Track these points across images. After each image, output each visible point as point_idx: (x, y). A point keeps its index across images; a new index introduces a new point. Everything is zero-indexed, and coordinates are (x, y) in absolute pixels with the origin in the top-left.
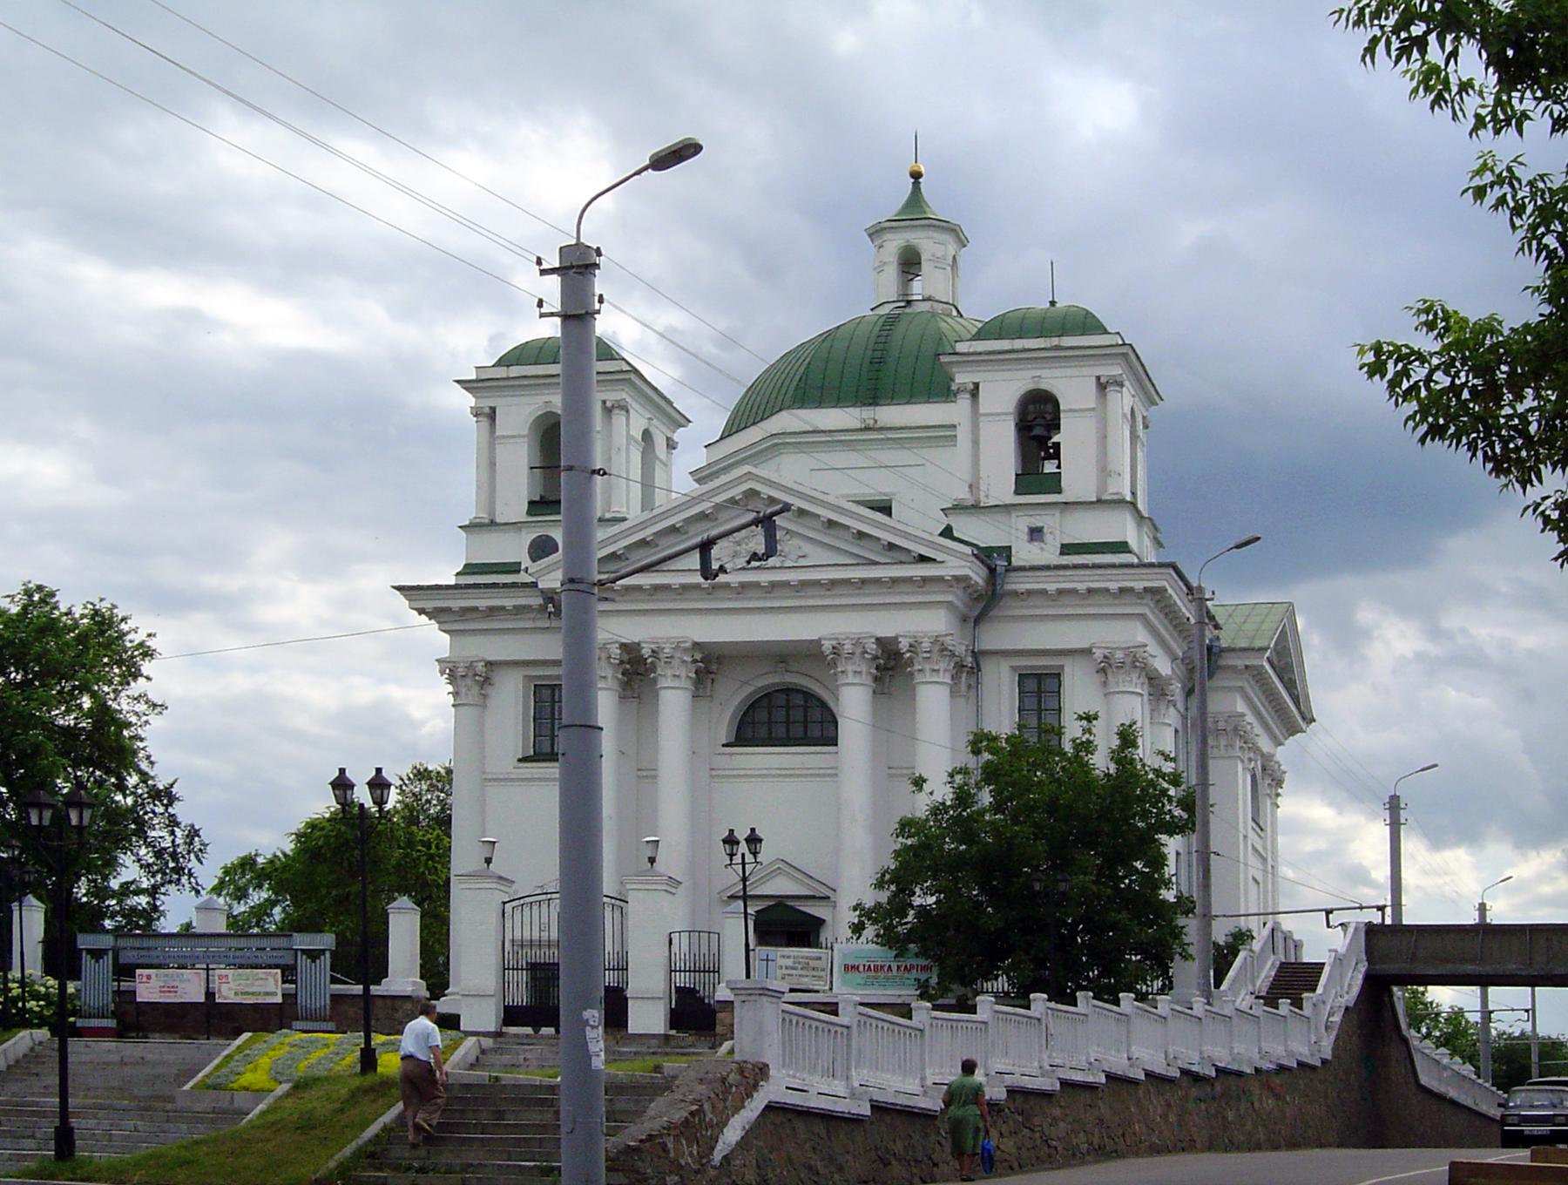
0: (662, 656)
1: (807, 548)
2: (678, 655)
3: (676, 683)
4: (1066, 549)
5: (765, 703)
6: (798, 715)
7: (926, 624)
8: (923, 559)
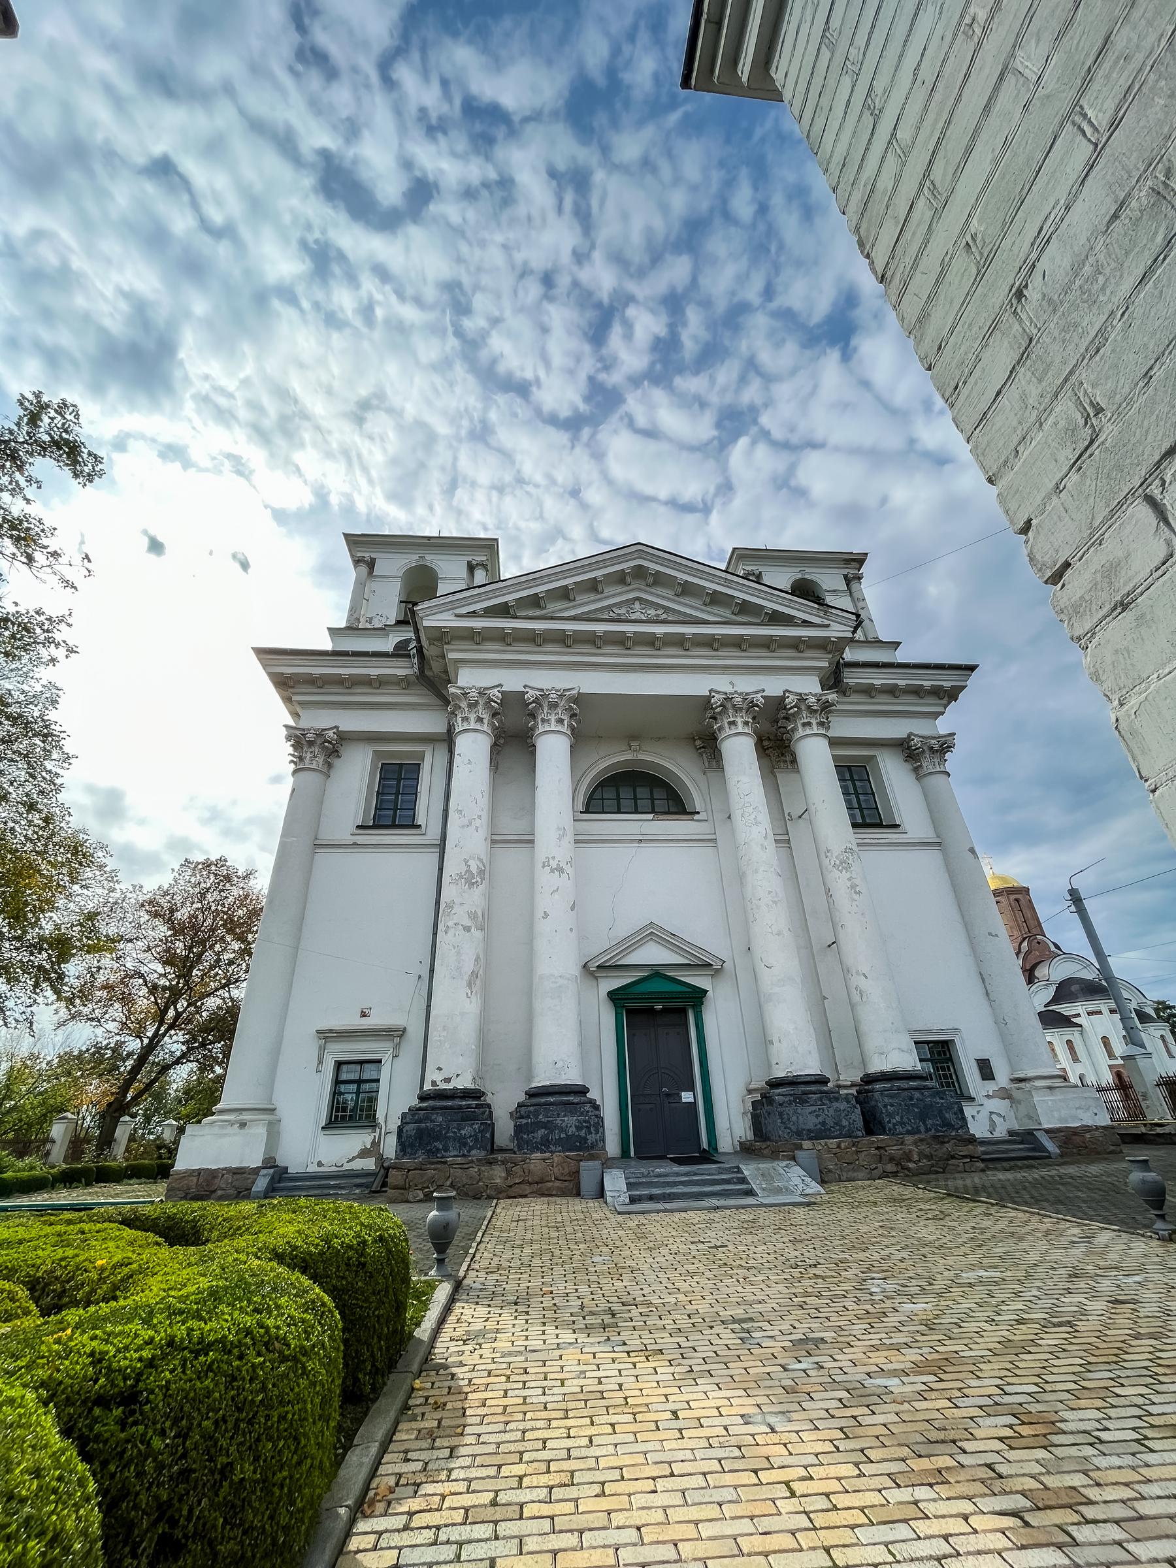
0: (545, 705)
3: (560, 728)
7: (809, 686)
8: (806, 623)
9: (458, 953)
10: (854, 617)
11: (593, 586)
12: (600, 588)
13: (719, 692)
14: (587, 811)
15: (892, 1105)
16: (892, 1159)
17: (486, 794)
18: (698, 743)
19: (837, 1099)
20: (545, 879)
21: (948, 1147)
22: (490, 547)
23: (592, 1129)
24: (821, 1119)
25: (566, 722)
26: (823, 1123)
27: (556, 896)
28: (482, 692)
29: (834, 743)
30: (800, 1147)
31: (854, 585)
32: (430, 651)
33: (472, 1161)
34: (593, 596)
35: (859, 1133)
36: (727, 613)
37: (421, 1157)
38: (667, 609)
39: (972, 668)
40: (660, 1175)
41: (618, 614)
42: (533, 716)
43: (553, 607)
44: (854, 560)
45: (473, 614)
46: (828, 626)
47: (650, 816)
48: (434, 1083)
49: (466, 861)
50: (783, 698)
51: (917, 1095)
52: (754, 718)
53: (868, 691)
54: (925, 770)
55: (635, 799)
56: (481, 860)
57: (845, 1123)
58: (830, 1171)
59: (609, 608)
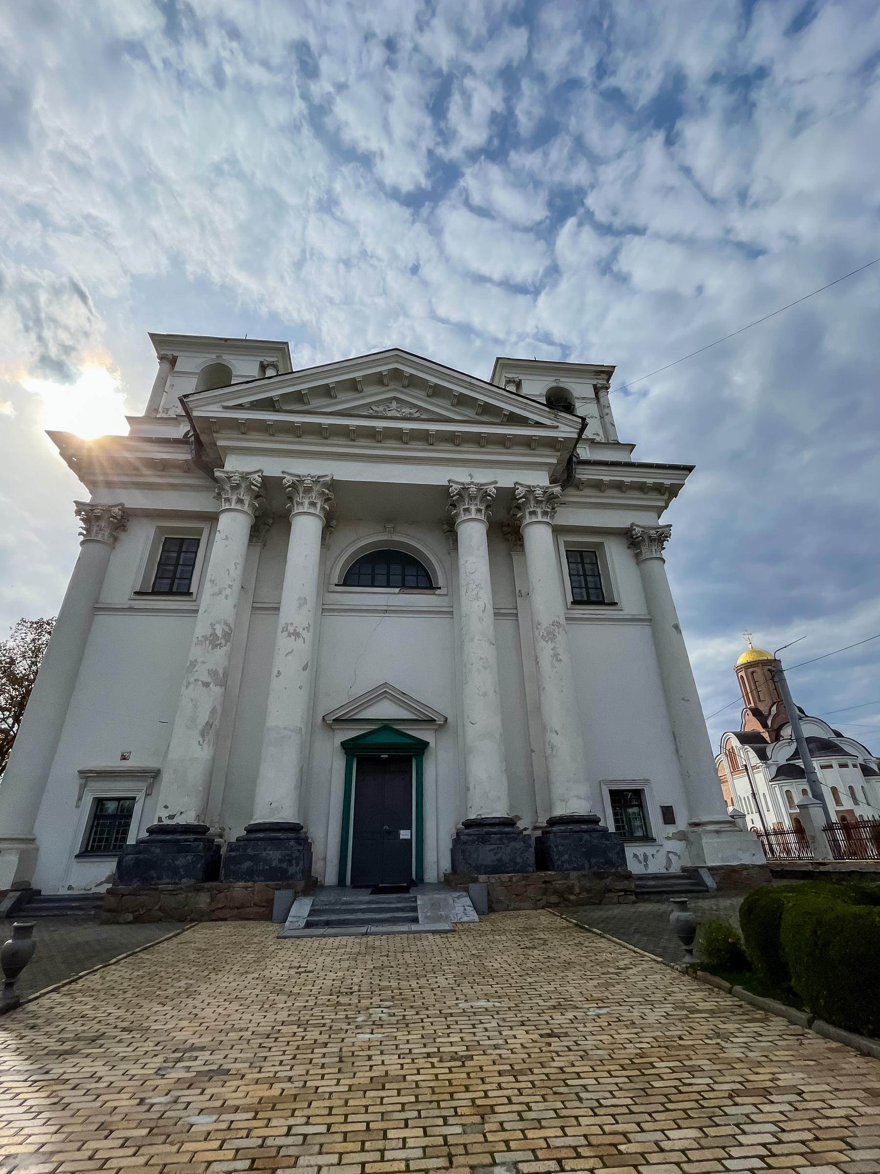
0: (301, 490)
2: (317, 488)
3: (312, 510)
8: (538, 424)
9: (195, 706)
10: (580, 420)
11: (354, 386)
12: (359, 387)
13: (457, 483)
15: (563, 845)
16: (556, 892)
17: (240, 568)
18: (445, 527)
19: (515, 839)
20: (284, 643)
21: (608, 881)
22: (281, 349)
23: (294, 862)
24: (498, 856)
25: (319, 506)
26: (500, 860)
27: (290, 657)
28: (245, 477)
29: (558, 530)
30: (475, 880)
31: (602, 394)
32: (204, 438)
33: (181, 888)
34: (351, 395)
35: (531, 869)
36: (470, 413)
37: (136, 884)
38: (420, 409)
39: (690, 469)
40: (346, 903)
41: (376, 412)
42: (290, 499)
43: (316, 403)
44: (603, 372)
45: (240, 407)
46: (557, 427)
47: (397, 590)
48: (160, 819)
49: (212, 625)
50: (514, 490)
51: (586, 836)
52: (488, 507)
53: (598, 486)
54: (644, 556)
55: (388, 574)
56: (227, 624)
57: (519, 860)
58: (501, 901)
59: (369, 405)
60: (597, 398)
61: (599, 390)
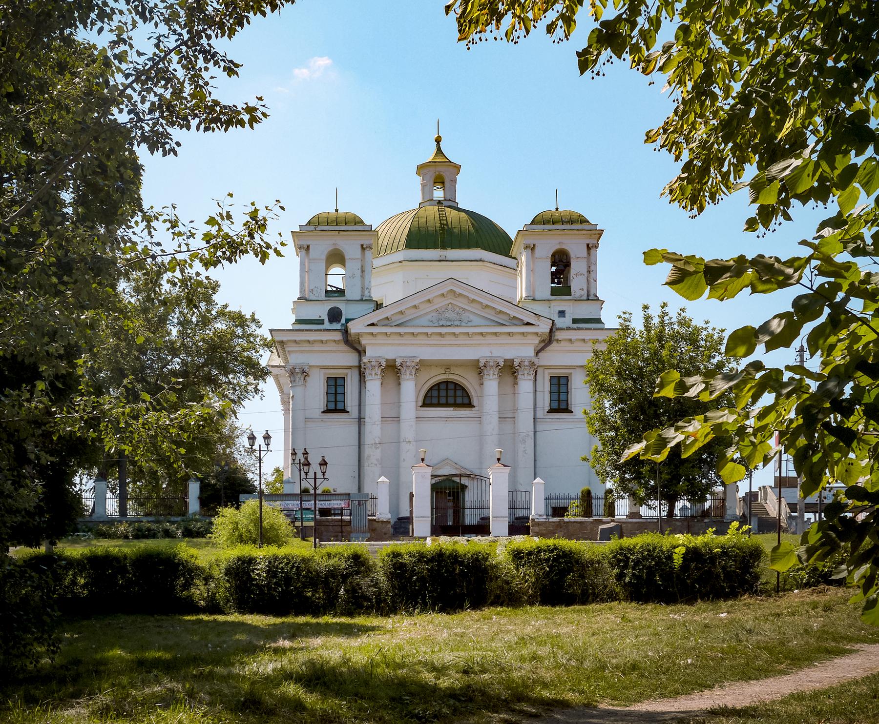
1: (472, 317)
4: (575, 321)
5: (436, 387)
6: (451, 393)
8: (528, 324)
14: (425, 405)
31: (592, 251)
45: (373, 324)
60: (589, 254)
61: (591, 248)
